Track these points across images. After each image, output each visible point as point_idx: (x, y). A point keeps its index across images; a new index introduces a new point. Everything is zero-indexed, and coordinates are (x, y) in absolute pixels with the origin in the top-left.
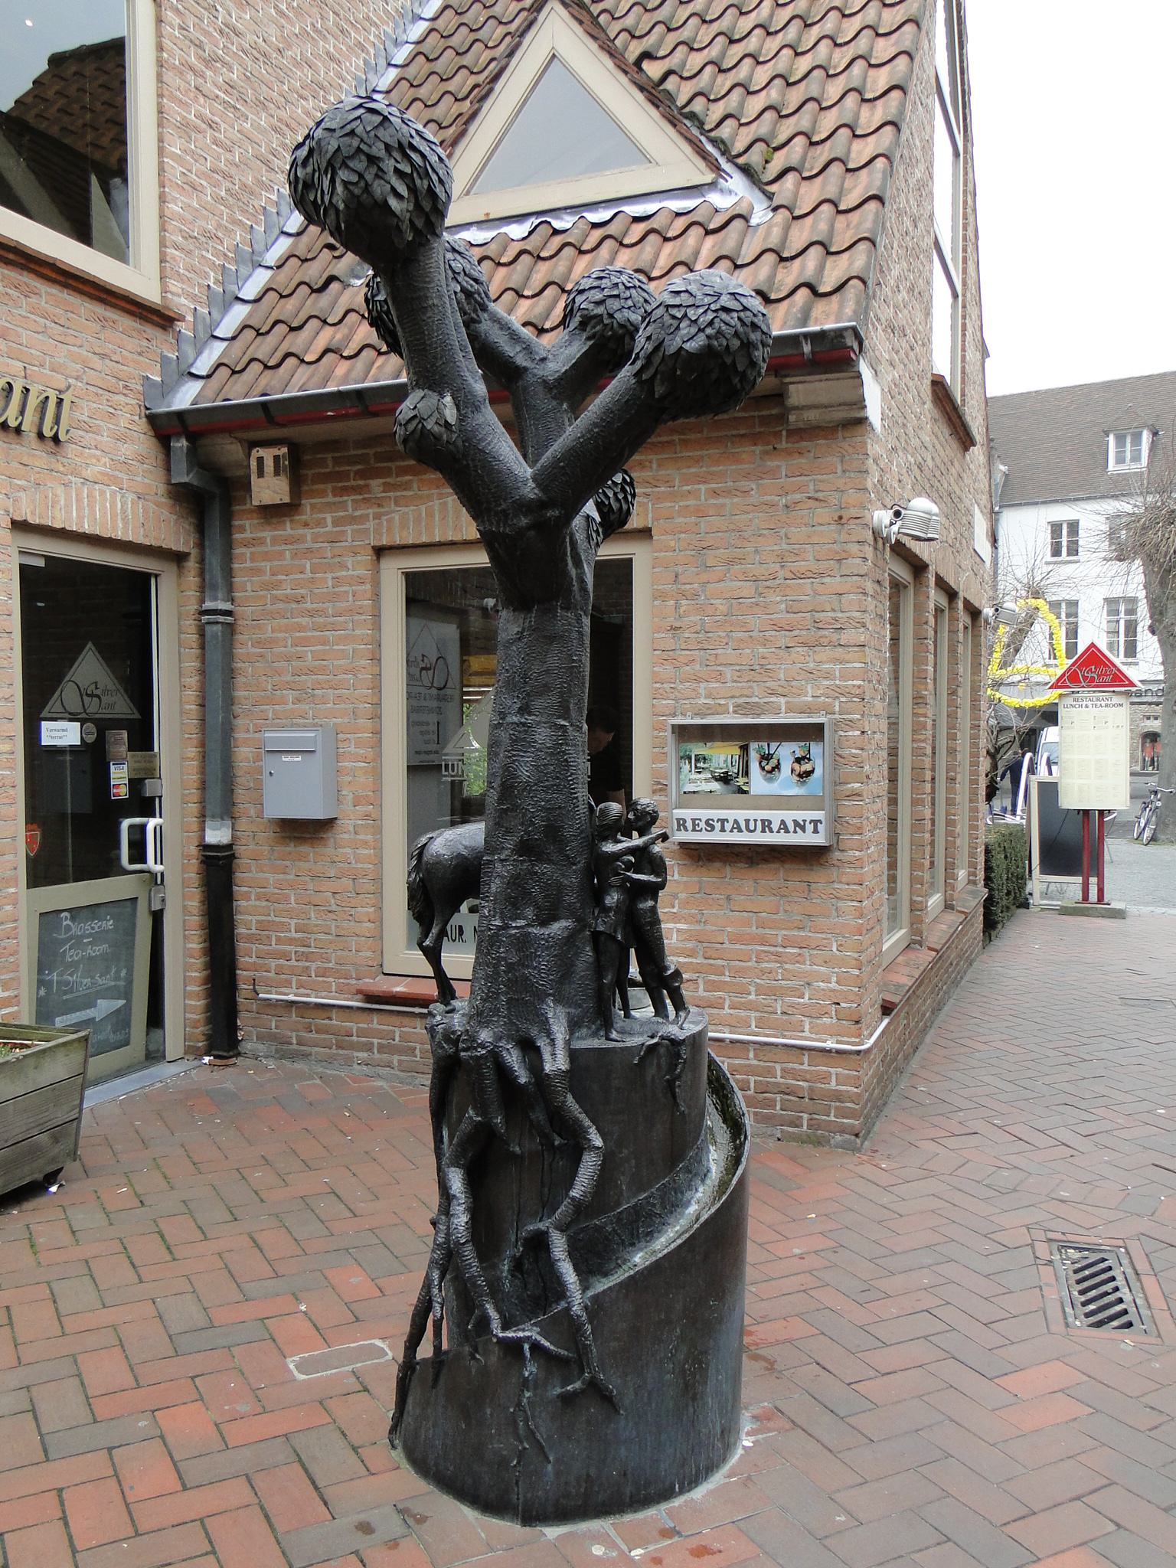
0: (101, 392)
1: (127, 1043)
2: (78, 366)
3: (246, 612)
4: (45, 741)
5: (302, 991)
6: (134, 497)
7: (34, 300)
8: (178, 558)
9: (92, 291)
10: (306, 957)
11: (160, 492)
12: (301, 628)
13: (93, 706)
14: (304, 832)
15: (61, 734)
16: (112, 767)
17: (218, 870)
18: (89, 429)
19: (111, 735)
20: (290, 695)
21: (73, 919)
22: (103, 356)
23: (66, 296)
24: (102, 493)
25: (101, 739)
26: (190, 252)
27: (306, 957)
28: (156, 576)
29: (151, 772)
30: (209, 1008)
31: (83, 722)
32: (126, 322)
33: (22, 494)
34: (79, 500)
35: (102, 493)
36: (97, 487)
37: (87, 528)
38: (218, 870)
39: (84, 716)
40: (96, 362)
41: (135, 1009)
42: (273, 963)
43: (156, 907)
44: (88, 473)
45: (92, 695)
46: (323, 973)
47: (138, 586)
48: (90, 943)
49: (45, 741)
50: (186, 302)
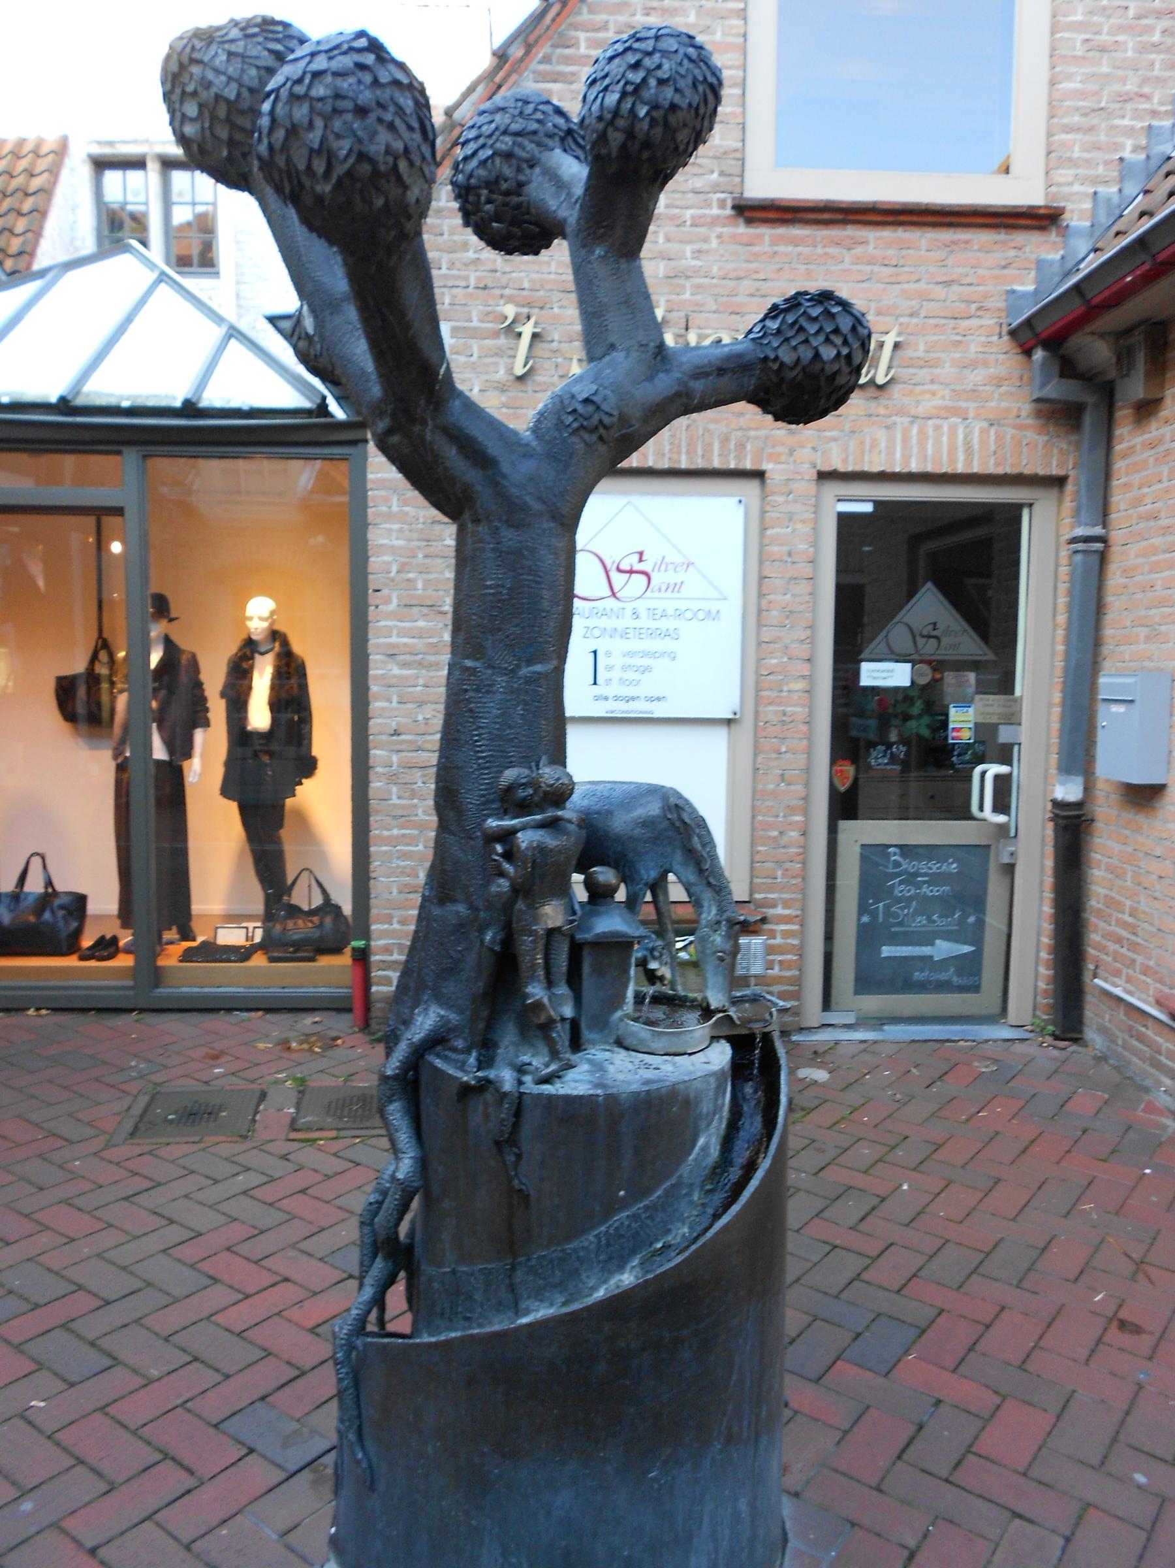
0: (943, 321)
1: (976, 988)
2: (914, 303)
3: (1116, 536)
4: (865, 681)
5: (1129, 987)
6: (985, 425)
7: (859, 250)
8: (1059, 482)
9: (880, 218)
10: (1133, 946)
11: (1024, 413)
12: (1155, 551)
13: (929, 648)
14: (1144, 796)
15: (884, 674)
16: (952, 711)
17: (1072, 829)
18: (927, 364)
19: (949, 678)
20: (1142, 632)
21: (903, 855)
22: (947, 283)
23: (900, 233)
24: (937, 428)
25: (935, 683)
26: (1091, 129)
27: (1133, 946)
28: (1030, 505)
29: (1013, 719)
30: (1055, 980)
31: (914, 663)
32: (980, 238)
33: (833, 445)
34: (906, 440)
35: (937, 428)
36: (930, 422)
37: (914, 467)
38: (1072, 829)
39: (915, 657)
40: (939, 292)
41: (986, 962)
42: (1113, 947)
43: (1006, 860)
44: (921, 410)
45: (929, 637)
46: (1146, 971)
47: (1006, 520)
48: (924, 882)
49: (865, 681)
50: (1082, 189)
